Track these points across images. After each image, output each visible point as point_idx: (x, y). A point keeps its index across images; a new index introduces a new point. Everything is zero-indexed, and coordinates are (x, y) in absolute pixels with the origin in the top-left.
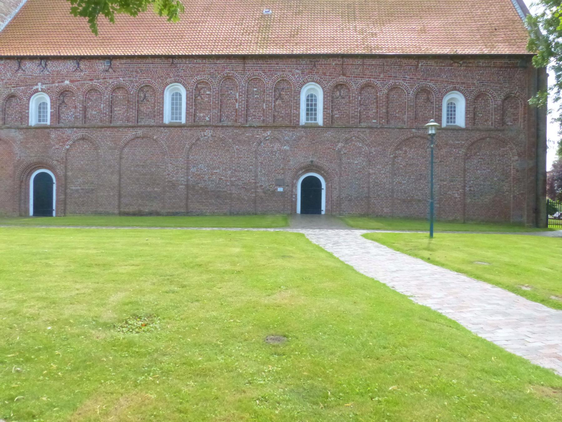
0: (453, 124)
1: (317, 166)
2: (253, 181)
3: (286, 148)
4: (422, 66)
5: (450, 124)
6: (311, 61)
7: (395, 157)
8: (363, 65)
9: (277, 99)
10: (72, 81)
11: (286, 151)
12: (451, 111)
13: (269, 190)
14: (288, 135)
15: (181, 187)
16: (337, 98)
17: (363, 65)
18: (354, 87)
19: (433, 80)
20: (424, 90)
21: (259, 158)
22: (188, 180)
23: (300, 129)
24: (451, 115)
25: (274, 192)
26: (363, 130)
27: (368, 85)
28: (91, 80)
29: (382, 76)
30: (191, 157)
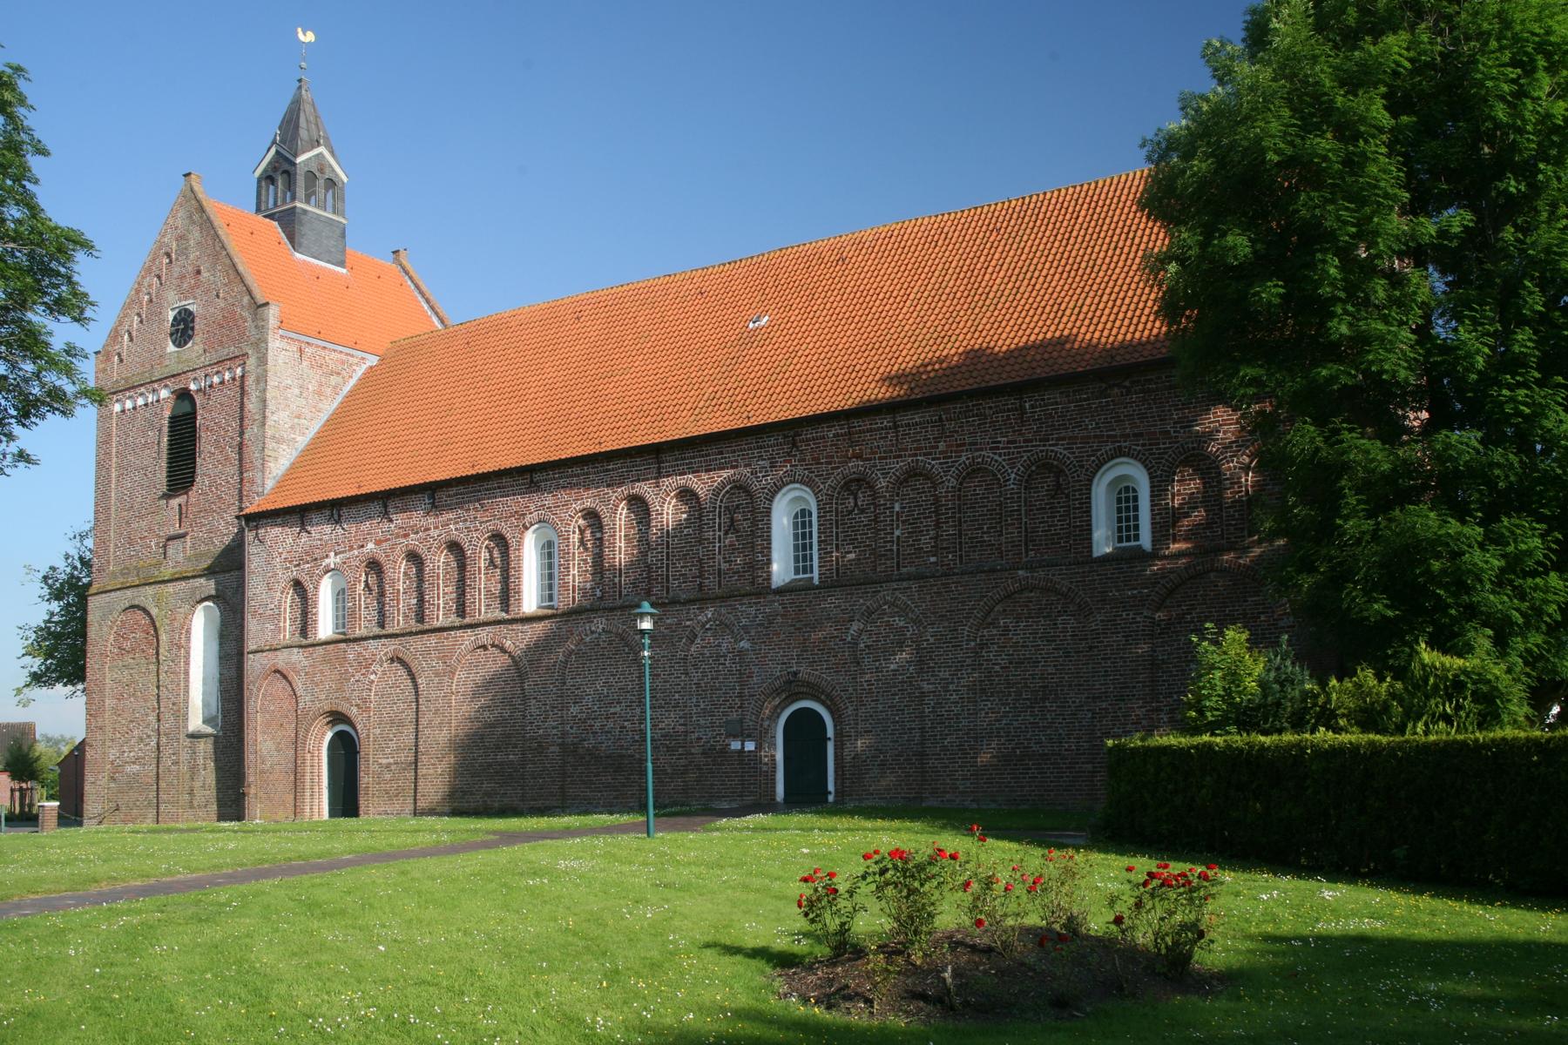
0: (1133, 543)
1: (809, 684)
2: (682, 728)
3: (744, 644)
4: (1032, 407)
5: (1125, 544)
6: (785, 437)
7: (982, 646)
8: (896, 427)
9: (726, 533)
10: (378, 543)
11: (741, 652)
12: (1128, 509)
13: (713, 748)
14: (747, 611)
15: (552, 749)
16: (850, 512)
17: (896, 427)
18: (882, 483)
19: (1063, 439)
20: (1046, 466)
21: (691, 670)
22: (564, 734)
23: (770, 597)
24: (1128, 519)
25: (725, 751)
26: (905, 584)
27: (913, 474)
28: (406, 536)
29: (942, 446)
30: (569, 682)
